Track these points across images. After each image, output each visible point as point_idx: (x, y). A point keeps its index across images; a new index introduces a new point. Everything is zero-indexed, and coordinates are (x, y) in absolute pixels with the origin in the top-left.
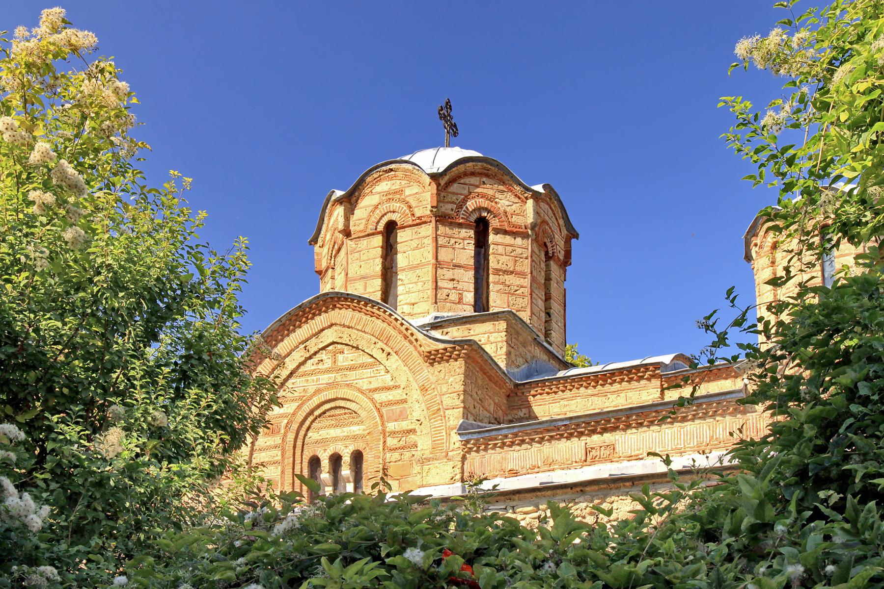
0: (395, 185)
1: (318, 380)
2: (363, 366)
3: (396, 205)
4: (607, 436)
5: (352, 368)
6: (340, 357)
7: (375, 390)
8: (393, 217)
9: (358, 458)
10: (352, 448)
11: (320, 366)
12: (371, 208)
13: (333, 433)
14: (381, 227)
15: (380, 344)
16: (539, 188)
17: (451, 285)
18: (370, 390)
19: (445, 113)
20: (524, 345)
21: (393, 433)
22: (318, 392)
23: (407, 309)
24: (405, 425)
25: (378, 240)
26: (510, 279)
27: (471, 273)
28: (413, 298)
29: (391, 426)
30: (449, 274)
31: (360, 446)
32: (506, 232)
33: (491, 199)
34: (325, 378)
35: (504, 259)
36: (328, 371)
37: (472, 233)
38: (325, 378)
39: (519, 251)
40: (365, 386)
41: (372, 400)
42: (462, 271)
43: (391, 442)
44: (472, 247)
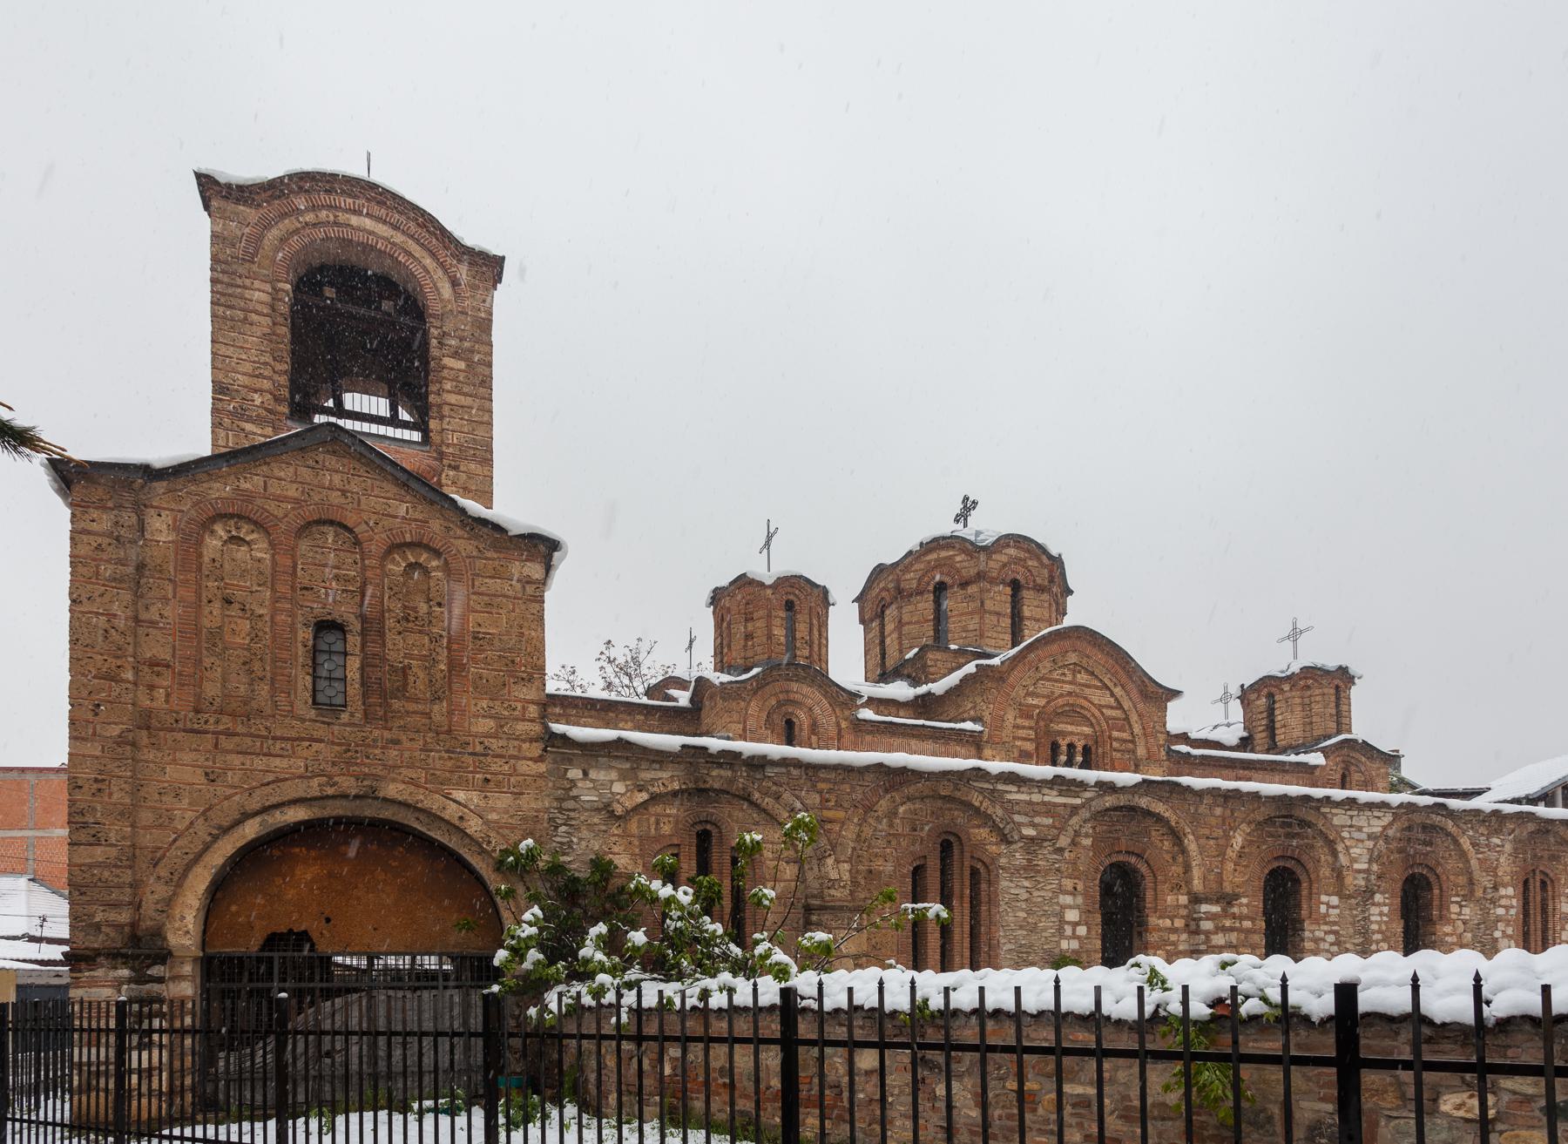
1: (1062, 687)
7: (1103, 706)
22: (1061, 696)
38: (1068, 687)
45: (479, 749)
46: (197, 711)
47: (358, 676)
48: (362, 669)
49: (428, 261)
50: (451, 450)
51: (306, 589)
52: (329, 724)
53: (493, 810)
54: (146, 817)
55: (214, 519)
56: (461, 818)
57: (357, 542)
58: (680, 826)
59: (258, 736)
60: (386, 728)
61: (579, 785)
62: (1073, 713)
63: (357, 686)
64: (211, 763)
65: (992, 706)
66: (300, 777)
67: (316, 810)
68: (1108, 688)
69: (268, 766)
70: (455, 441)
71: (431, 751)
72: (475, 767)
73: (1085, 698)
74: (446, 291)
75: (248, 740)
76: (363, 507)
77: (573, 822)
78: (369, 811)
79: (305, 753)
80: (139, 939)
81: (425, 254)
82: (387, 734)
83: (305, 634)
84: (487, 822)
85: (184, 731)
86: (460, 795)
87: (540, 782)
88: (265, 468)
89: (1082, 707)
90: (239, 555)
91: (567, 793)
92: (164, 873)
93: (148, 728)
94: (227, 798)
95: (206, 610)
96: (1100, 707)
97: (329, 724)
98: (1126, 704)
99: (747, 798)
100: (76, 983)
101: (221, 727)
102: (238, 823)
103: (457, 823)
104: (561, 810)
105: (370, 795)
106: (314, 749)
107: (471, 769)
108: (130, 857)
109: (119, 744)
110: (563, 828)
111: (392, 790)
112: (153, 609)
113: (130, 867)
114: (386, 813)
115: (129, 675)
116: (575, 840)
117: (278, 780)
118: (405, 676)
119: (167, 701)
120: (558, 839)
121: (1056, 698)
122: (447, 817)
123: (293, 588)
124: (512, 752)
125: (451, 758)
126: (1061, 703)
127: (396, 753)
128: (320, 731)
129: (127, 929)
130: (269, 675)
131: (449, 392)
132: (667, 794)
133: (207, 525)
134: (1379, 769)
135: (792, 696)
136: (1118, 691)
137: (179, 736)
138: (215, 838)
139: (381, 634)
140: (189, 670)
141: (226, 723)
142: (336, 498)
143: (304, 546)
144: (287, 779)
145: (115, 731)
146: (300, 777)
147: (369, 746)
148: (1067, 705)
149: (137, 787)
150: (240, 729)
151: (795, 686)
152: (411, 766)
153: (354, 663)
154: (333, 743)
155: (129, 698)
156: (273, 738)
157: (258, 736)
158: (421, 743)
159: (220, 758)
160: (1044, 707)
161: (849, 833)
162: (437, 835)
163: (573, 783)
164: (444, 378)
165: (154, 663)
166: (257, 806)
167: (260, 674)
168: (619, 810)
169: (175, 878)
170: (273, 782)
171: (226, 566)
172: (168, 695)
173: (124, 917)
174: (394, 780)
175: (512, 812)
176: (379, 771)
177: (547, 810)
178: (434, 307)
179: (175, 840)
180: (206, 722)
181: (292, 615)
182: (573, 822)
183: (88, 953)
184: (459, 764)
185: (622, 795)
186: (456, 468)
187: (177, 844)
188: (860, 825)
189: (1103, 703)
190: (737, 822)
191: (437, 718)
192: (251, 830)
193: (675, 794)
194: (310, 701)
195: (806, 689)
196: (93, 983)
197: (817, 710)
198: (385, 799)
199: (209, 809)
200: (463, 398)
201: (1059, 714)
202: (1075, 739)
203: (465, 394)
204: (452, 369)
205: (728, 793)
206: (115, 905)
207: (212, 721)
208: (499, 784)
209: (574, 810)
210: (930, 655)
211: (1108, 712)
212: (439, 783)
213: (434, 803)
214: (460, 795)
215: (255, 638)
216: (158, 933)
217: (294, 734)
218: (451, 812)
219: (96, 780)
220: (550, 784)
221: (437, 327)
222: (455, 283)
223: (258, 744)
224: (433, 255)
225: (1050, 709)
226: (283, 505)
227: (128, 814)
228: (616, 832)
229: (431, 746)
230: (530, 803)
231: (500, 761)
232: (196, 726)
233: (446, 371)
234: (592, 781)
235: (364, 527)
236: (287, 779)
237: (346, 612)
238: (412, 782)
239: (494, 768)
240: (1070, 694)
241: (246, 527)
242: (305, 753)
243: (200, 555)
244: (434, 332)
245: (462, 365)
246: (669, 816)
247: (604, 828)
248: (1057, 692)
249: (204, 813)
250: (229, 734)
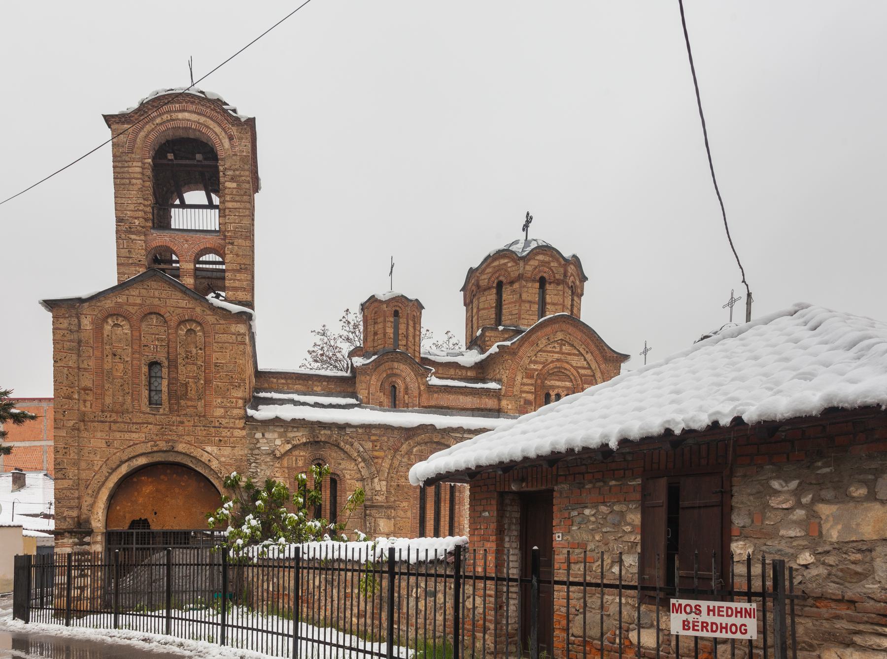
2: (574, 355)
5: (569, 354)
6: (564, 347)
8: (545, 275)
12: (533, 267)
14: (538, 278)
15: (583, 346)
18: (577, 367)
22: (552, 362)
25: (537, 285)
34: (556, 356)
36: (557, 353)
45: (217, 424)
46: (103, 412)
47: (166, 389)
48: (168, 385)
49: (218, 129)
50: (230, 234)
51: (145, 346)
52: (154, 415)
53: (223, 456)
54: (83, 465)
55: (107, 317)
56: (209, 460)
57: (166, 322)
58: (307, 462)
59: (126, 423)
60: (178, 416)
61: (261, 441)
63: (166, 394)
64: (108, 437)
65: (508, 371)
66: (143, 442)
67: (149, 458)
68: (582, 355)
69: (130, 437)
70: (232, 229)
71: (197, 426)
72: (215, 434)
74: (226, 143)
75: (122, 425)
76: (168, 304)
77: (258, 461)
78: (172, 458)
79: (145, 430)
80: (81, 524)
81: (216, 125)
82: (178, 419)
83: (145, 369)
84: (220, 462)
85: (98, 422)
86: (209, 449)
87: (243, 440)
88: (127, 292)
90: (118, 332)
91: (254, 446)
92: (90, 492)
93: (84, 421)
94: (115, 454)
95: (106, 360)
96: (576, 368)
97: (154, 415)
98: (594, 365)
99: (338, 446)
100: (57, 545)
101: (112, 419)
102: (119, 466)
103: (207, 462)
104: (252, 454)
105: (172, 450)
106: (148, 428)
107: (213, 435)
108: (77, 486)
109: (72, 430)
110: (253, 465)
111: (181, 447)
112: (85, 362)
113: (77, 489)
114: (179, 459)
115: (76, 396)
116: (259, 470)
117: (134, 444)
118: (187, 388)
119: (91, 408)
120: (251, 470)
121: (549, 364)
122: (203, 460)
123: (140, 346)
124: (232, 425)
125: (205, 430)
126: (552, 367)
127: (182, 428)
128: (151, 419)
129: (76, 519)
130: (131, 391)
131: (228, 201)
132: (301, 444)
133: (105, 320)
135: (395, 371)
136: (589, 357)
137: (96, 424)
138: (110, 474)
139: (177, 368)
140: (99, 392)
141: (114, 417)
142: (156, 302)
143: (144, 326)
144: (137, 444)
145: (71, 423)
146: (143, 442)
147: (171, 425)
148: (556, 368)
149: (80, 450)
150: (120, 420)
151: (396, 365)
152: (188, 435)
153: (165, 383)
154: (156, 424)
155: (76, 407)
156: (133, 423)
157: (126, 423)
158: (192, 422)
159: (111, 434)
160: (541, 370)
161: (386, 465)
162: (199, 469)
163: (258, 440)
164: (226, 194)
165: (85, 389)
166: (126, 458)
167: (127, 391)
168: (278, 455)
169: (95, 494)
170: (132, 445)
171: (113, 338)
172: (91, 404)
173: (75, 513)
174: (181, 442)
175: (231, 457)
176: (175, 438)
177: (246, 455)
178: (221, 154)
179: (94, 476)
180: (106, 417)
181: (140, 361)
182: (258, 461)
183: (62, 531)
184: (209, 432)
185: (280, 446)
186: (232, 244)
187: (96, 477)
188: (392, 460)
189: (579, 365)
190: (333, 459)
191: (200, 409)
192: (124, 469)
193: (305, 444)
194: (148, 403)
195: (402, 366)
196: (63, 545)
197: (408, 379)
198: (177, 452)
199: (108, 459)
200: (235, 204)
203: (237, 201)
204: (230, 188)
205: (329, 443)
206: (71, 508)
207: (108, 416)
208: (225, 442)
209: (258, 455)
210: (487, 334)
211: (582, 371)
212: (200, 443)
213: (197, 453)
214: (209, 449)
215: (125, 373)
216: (88, 521)
217: (140, 421)
218: (205, 458)
219: (64, 448)
220: (248, 441)
221: (222, 165)
222: (231, 138)
223: (127, 426)
224: (220, 125)
225: (545, 371)
226: (135, 308)
227: (76, 464)
228: (277, 466)
229: (196, 424)
230: (240, 452)
231: (226, 430)
232: (102, 419)
233: (227, 190)
234: (266, 439)
235: (168, 314)
236: (137, 444)
237: (162, 357)
238: (189, 443)
239: (224, 434)
240: (558, 360)
241: (120, 319)
242: (145, 430)
243: (103, 334)
244: (221, 168)
245: (234, 185)
246: (301, 456)
247: (272, 463)
248: (550, 360)
249: (105, 462)
250: (115, 422)
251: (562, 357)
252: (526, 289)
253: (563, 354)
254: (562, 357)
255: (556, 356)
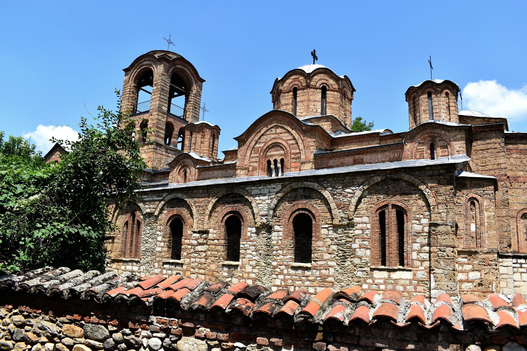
0: (297, 76)
2: (284, 133)
3: (297, 83)
4: (360, 156)
5: (281, 133)
9: (282, 161)
10: (280, 158)
11: (272, 132)
13: (275, 153)
16: (342, 77)
17: (313, 107)
19: (314, 54)
20: (337, 125)
21: (293, 154)
23: (300, 114)
24: (298, 151)
25: (291, 93)
26: (333, 105)
27: (320, 103)
28: (301, 111)
29: (293, 151)
30: (313, 104)
31: (283, 157)
32: (333, 91)
33: (327, 80)
34: (273, 136)
35: (331, 98)
37: (321, 91)
39: (336, 96)
40: (285, 138)
41: (288, 143)
42: (317, 102)
43: (292, 156)
44: (320, 95)
62: (276, 145)
73: (280, 139)
89: (279, 143)
96: (286, 141)
98: (297, 136)
134: (455, 136)
136: (293, 132)
201: (270, 148)
202: (277, 158)
248: (269, 139)
251: (277, 136)
252: (284, 98)
253: (277, 134)
254: (277, 136)
255: (273, 136)
